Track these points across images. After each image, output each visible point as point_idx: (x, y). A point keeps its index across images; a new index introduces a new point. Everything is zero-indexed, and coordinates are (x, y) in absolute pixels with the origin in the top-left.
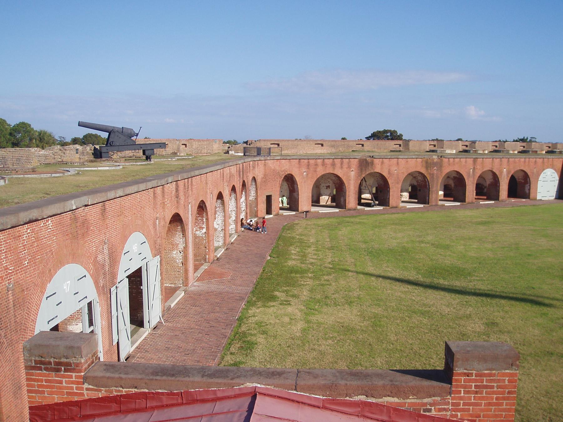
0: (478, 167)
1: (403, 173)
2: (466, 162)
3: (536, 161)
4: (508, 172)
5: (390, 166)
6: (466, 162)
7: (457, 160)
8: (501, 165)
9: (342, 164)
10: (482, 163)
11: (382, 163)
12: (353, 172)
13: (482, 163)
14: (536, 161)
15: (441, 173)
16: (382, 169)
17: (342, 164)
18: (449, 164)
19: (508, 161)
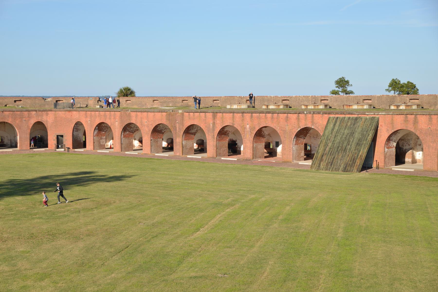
0: (218, 122)
1: (152, 125)
2: (205, 116)
3: (287, 117)
4: (252, 129)
5: (141, 118)
6: (205, 116)
7: (197, 114)
8: (243, 120)
9: (110, 116)
10: (222, 118)
11: (137, 116)
12: (117, 123)
13: (222, 118)
14: (287, 117)
15: (183, 126)
16: (136, 120)
17: (110, 116)
18: (190, 118)
19: (252, 117)
